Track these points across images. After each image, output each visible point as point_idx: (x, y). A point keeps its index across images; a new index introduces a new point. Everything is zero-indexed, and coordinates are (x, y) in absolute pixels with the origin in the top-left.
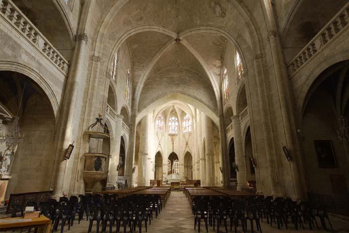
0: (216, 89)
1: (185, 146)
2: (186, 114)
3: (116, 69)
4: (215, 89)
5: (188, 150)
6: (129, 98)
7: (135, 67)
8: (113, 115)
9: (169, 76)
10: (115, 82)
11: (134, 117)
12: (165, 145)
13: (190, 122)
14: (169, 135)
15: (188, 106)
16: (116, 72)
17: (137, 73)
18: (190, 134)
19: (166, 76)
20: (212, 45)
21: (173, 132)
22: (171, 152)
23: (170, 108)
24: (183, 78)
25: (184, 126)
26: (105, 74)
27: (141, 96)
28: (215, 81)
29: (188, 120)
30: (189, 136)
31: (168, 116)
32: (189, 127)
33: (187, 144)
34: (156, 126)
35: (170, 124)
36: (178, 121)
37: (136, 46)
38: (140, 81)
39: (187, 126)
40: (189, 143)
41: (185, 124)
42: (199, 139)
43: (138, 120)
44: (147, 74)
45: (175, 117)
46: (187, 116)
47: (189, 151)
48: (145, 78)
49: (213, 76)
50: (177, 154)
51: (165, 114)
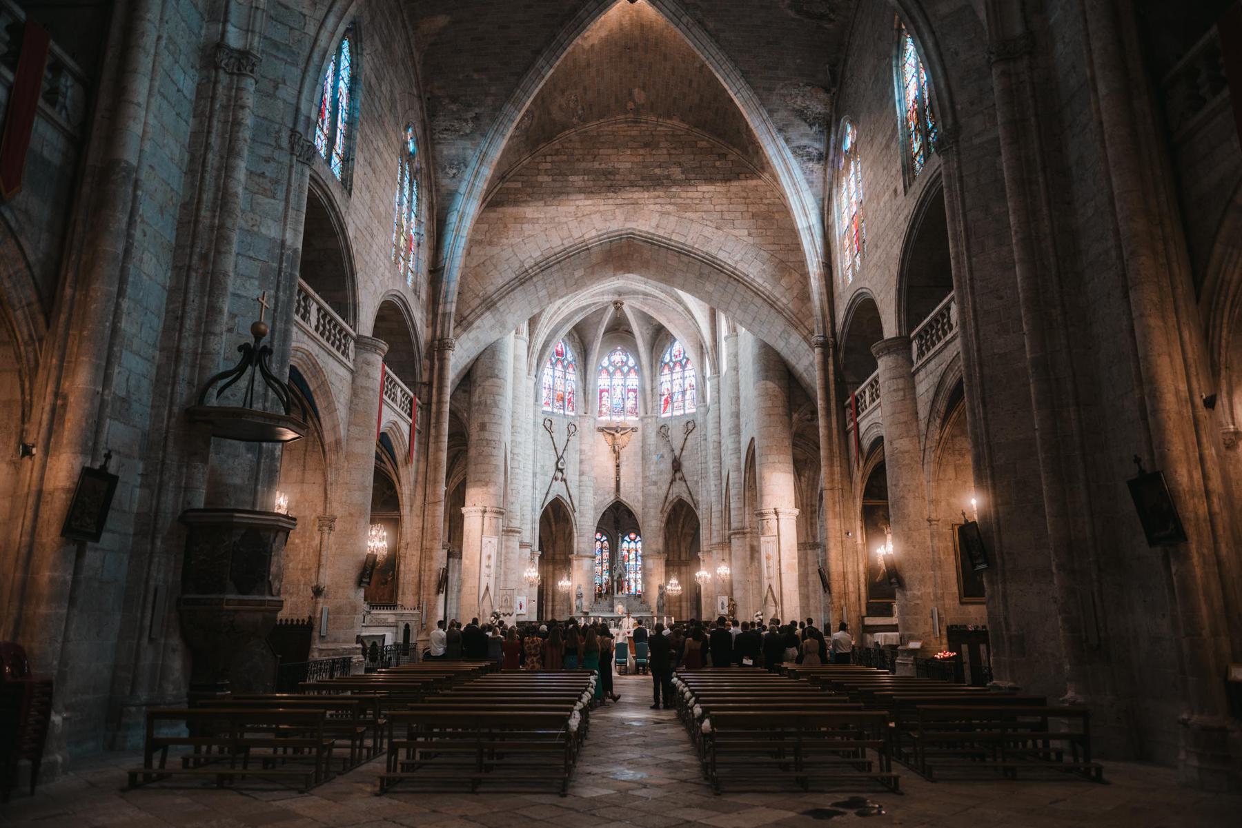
0: (805, 218)
2: (670, 338)
3: (350, 124)
4: (801, 223)
5: (679, 490)
6: (417, 261)
7: (442, 122)
8: (336, 337)
9: (596, 165)
10: (347, 183)
11: (439, 347)
13: (691, 373)
14: (601, 430)
15: (679, 301)
16: (349, 137)
17: (448, 150)
18: (690, 426)
19: (583, 165)
20: (791, 14)
21: (617, 419)
22: (610, 499)
23: (605, 309)
24: (658, 171)
25: (665, 388)
26: (285, 143)
27: (469, 253)
28: (804, 186)
29: (683, 367)
31: (597, 346)
32: (684, 393)
33: (677, 466)
34: (545, 393)
35: (603, 381)
36: (639, 370)
37: (441, 20)
38: (463, 188)
39: (677, 389)
40: (687, 465)
41: (669, 381)
42: (728, 443)
43: (457, 359)
44: (496, 154)
45: (624, 351)
46: (677, 347)
47: (685, 496)
48: (487, 172)
49: (794, 163)
50: (636, 508)
51: (581, 337)
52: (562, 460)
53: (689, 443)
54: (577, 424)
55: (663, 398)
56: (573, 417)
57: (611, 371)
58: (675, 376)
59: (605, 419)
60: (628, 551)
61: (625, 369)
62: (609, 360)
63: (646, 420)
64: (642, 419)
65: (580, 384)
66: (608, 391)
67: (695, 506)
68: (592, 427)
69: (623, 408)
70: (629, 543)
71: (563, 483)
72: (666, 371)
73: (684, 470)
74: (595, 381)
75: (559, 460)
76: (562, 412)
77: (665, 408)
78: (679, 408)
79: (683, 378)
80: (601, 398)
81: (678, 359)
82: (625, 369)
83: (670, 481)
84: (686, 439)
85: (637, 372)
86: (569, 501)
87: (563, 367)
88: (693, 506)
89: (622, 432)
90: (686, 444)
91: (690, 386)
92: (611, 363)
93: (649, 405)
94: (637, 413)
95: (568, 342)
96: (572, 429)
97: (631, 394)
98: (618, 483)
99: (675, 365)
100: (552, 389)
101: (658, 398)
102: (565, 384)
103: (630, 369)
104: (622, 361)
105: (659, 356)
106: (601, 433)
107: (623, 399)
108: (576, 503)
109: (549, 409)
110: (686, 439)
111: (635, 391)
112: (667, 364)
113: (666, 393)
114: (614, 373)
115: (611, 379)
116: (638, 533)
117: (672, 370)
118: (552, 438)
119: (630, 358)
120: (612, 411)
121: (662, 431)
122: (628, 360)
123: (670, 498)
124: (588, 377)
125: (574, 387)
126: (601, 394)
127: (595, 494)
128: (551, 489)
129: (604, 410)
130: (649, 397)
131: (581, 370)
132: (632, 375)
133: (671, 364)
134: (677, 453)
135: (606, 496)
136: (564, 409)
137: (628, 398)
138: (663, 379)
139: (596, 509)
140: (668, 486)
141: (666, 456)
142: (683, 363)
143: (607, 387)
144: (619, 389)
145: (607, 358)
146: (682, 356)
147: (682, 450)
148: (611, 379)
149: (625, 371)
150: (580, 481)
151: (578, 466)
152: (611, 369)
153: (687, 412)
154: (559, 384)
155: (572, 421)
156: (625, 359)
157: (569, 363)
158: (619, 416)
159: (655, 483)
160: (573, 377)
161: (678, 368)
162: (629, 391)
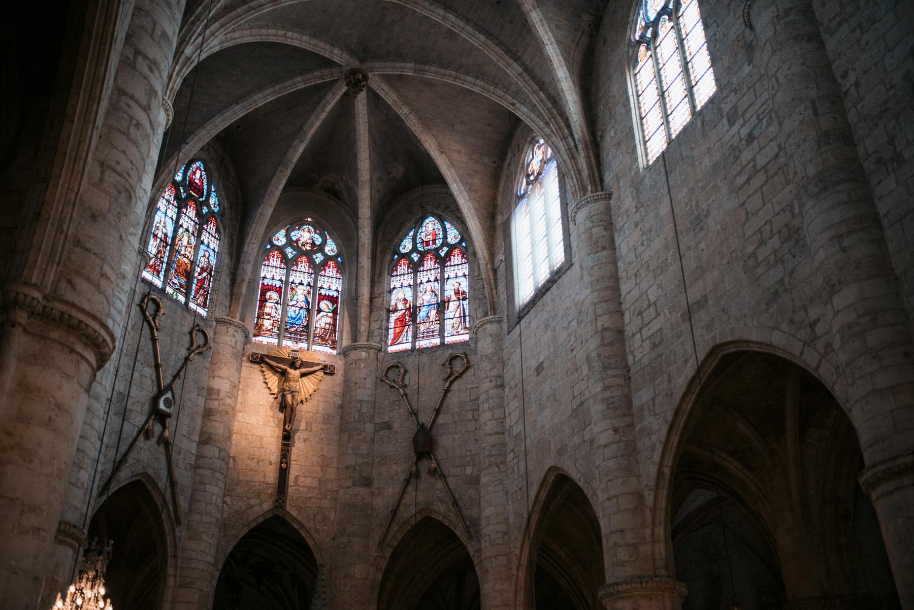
1: (399, 469)
29: (443, 262)
30: (452, 378)
32: (442, 306)
35: (271, 272)
39: (426, 298)
45: (319, 227)
47: (441, 510)
52: (169, 395)
53: (454, 399)
54: (210, 333)
55: (393, 317)
57: (290, 256)
58: (422, 277)
61: (319, 258)
62: (287, 236)
63: (354, 355)
64: (344, 353)
65: (226, 260)
66: (278, 290)
69: (307, 327)
71: (162, 449)
72: (403, 268)
73: (440, 454)
75: (160, 392)
76: (182, 299)
77: (397, 336)
78: (429, 334)
79: (442, 280)
80: (263, 301)
81: (432, 247)
83: (403, 477)
84: (447, 391)
85: (340, 268)
87: (199, 214)
88: (459, 532)
89: (303, 370)
90: (448, 401)
91: (457, 293)
92: (290, 242)
93: (363, 327)
94: (334, 342)
95: (216, 174)
96: (199, 340)
97: (324, 305)
99: (423, 255)
100: (170, 244)
101: (384, 314)
102: (196, 248)
103: (327, 258)
105: (391, 241)
106: (257, 367)
107: (308, 310)
108: (183, 503)
111: (333, 300)
112: (407, 256)
113: (400, 306)
114: (295, 261)
115: (288, 271)
117: (415, 268)
119: (330, 241)
120: (284, 329)
121: (391, 374)
122: (324, 243)
125: (213, 261)
126: (263, 293)
128: (132, 455)
129: (267, 324)
130: (364, 311)
131: (231, 236)
132: (331, 271)
133: (415, 257)
134: (425, 418)
135: (253, 502)
137: (319, 311)
138: (395, 282)
140: (398, 488)
141: (396, 426)
143: (278, 284)
144: (301, 292)
145: (283, 232)
146: (439, 242)
147: (438, 412)
148: (288, 271)
149: (318, 261)
150: (199, 456)
151: (199, 421)
153: (448, 340)
154: (185, 242)
155: (201, 323)
156: (318, 241)
157: (211, 213)
158: (297, 341)
160: (214, 244)
162: (322, 297)
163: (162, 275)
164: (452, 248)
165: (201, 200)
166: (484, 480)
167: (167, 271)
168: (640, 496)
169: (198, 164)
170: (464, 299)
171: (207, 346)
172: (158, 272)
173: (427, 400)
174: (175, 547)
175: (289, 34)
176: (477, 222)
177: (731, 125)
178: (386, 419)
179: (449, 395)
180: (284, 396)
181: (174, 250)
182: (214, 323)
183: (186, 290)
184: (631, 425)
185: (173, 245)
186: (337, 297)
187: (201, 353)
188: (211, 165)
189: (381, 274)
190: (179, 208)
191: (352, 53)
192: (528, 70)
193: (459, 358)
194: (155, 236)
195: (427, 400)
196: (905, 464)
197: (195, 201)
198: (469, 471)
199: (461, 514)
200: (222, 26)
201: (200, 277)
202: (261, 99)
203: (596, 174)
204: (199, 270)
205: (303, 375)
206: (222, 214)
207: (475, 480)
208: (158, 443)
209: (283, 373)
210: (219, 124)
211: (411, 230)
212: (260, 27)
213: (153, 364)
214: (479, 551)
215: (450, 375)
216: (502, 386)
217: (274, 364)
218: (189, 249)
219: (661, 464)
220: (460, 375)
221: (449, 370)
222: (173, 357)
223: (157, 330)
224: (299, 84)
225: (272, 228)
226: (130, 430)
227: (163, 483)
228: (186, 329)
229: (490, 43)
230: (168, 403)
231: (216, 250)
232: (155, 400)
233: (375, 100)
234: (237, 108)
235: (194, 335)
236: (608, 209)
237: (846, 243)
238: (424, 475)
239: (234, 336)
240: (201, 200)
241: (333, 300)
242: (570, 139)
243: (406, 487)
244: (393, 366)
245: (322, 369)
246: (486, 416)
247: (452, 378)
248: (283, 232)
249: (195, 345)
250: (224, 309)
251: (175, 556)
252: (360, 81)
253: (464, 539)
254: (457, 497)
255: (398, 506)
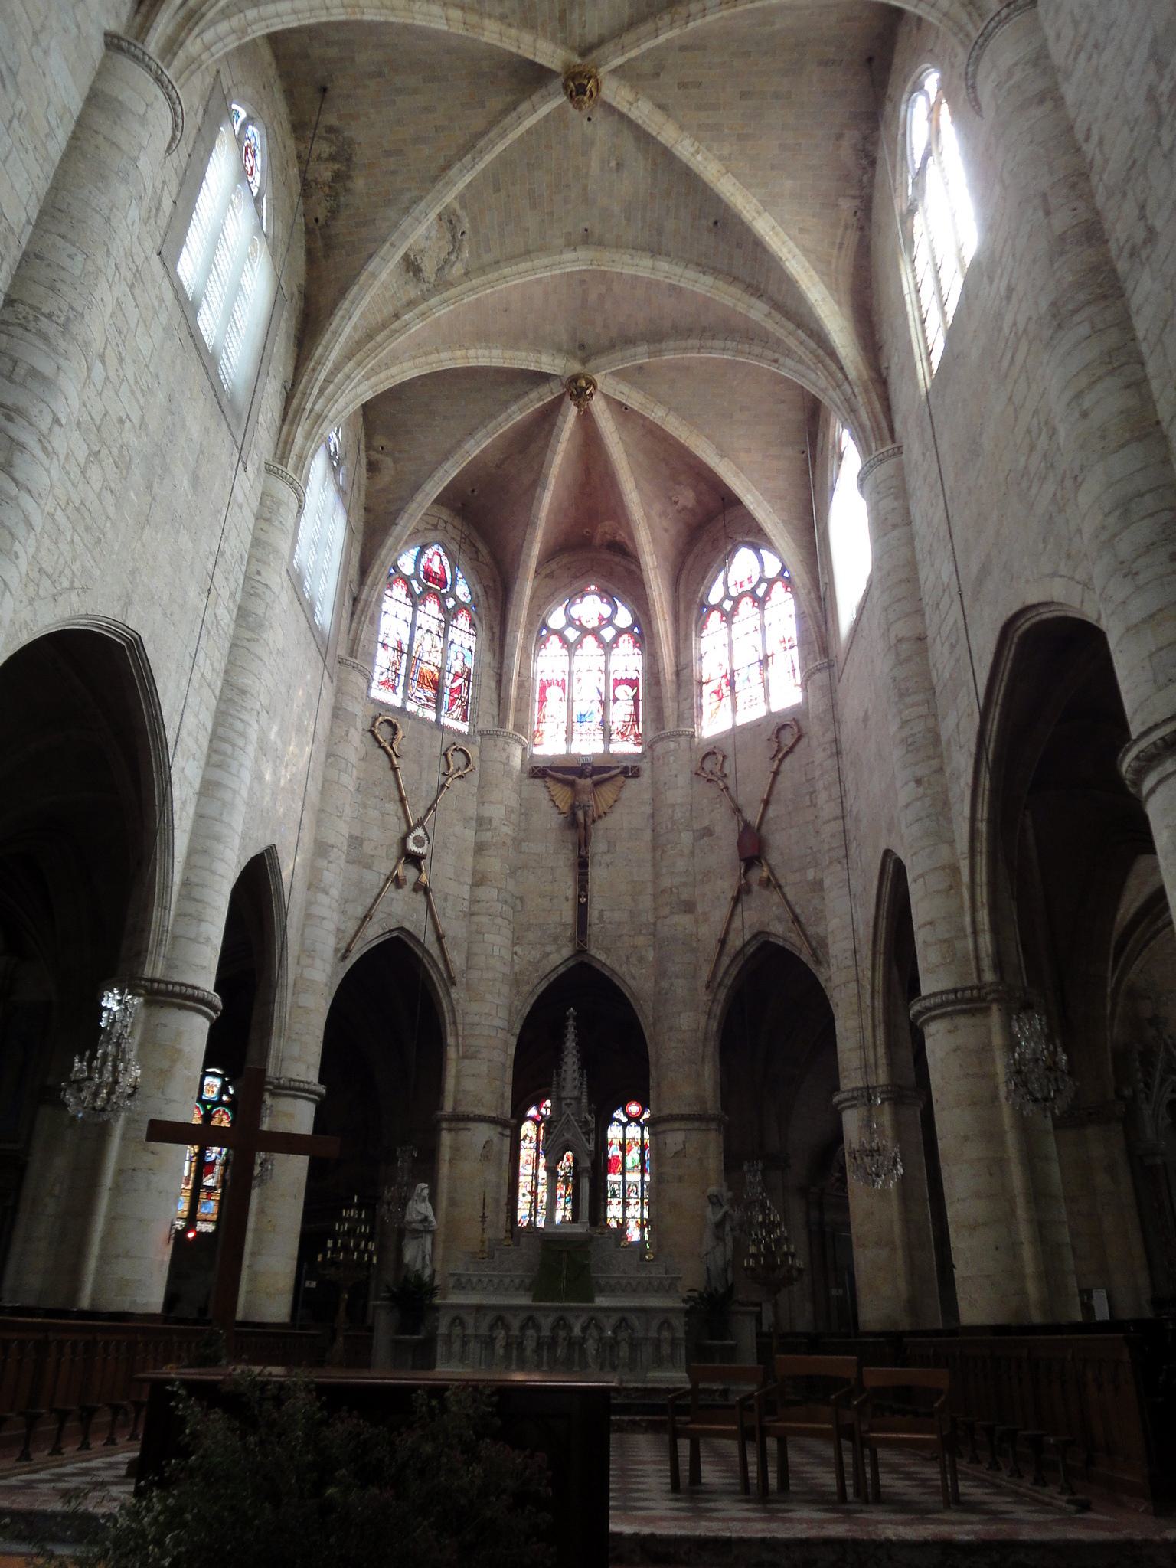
1: (726, 886)
12: (479, 880)
22: (560, 955)
29: (760, 602)
32: (764, 662)
34: (384, 658)
35: (550, 661)
36: (643, 634)
39: (746, 656)
40: (782, 843)
45: (606, 594)
52: (420, 832)
53: (784, 783)
54: (473, 752)
56: (460, 734)
59: (550, 745)
60: (623, 1147)
61: (608, 634)
65: (488, 658)
66: (562, 684)
67: (818, 962)
68: (517, 761)
70: (625, 1125)
71: (421, 897)
73: (774, 857)
74: (527, 657)
75: (410, 830)
76: (431, 715)
80: (543, 700)
81: (748, 587)
82: (608, 634)
83: (731, 893)
84: (776, 773)
86: (434, 950)
87: (443, 609)
88: (805, 957)
90: (779, 786)
92: (571, 622)
96: (457, 760)
98: (582, 910)
99: (737, 601)
103: (620, 632)
104: (601, 618)
105: (696, 592)
106: (538, 782)
108: (457, 959)
109: (395, 700)
110: (776, 773)
111: (632, 683)
112: (718, 607)
114: (579, 642)
116: (645, 1106)
117: (728, 617)
118: (394, 769)
123: (736, 942)
124: (508, 639)
125: (470, 664)
127: (517, 940)
132: (626, 644)
134: (752, 815)
135: (549, 949)
136: (438, 710)
137: (615, 700)
139: (516, 982)
140: (726, 910)
141: (718, 830)
142: (760, 592)
145: (561, 610)
146: (755, 580)
147: (766, 803)
150: (474, 901)
151: (469, 860)
152: (572, 634)
154: (427, 646)
156: (606, 611)
157: (460, 606)
159: (689, 907)
160: (470, 642)
161: (746, 604)
162: (618, 682)
163: (399, 690)
164: (771, 583)
165: (444, 591)
166: (827, 883)
167: (406, 686)
168: (955, 869)
169: (435, 548)
170: (792, 647)
171: (470, 767)
172: (394, 688)
173: (750, 793)
174: (453, 1011)
175: (472, 352)
176: (788, 539)
177: (991, 282)
178: (706, 823)
179: (779, 778)
180: (574, 814)
181: (413, 660)
182: (478, 738)
183: (436, 703)
184: (940, 770)
185: (409, 654)
186: (637, 679)
187: (460, 777)
188: (453, 547)
189: (688, 637)
190: (414, 606)
191: (569, 354)
192: (777, 306)
193: (788, 728)
194: (385, 646)
195: (750, 793)
196: (1162, 739)
197: (436, 594)
198: (811, 874)
199: (805, 935)
200: (359, 364)
201: (455, 685)
202: (476, 447)
203: (884, 424)
204: (451, 677)
205: (597, 784)
206: (475, 603)
207: (817, 886)
208: (415, 890)
209: (571, 784)
210: (434, 488)
211: (720, 572)
212: (426, 354)
213: (397, 797)
214: (829, 979)
215: (778, 751)
216: (838, 753)
217: (560, 775)
218: (435, 654)
219: (973, 819)
220: (791, 749)
221: (775, 746)
222: (425, 785)
223: (397, 756)
224: (518, 414)
225: (541, 605)
226: (374, 878)
227: (429, 939)
228: (438, 751)
229: (720, 284)
230: (419, 842)
231: (473, 649)
232: (404, 841)
233: (621, 409)
234: (447, 466)
235: (450, 756)
236: (900, 468)
237: (1087, 402)
238: (755, 888)
239: (504, 749)
240: (444, 591)
241: (632, 683)
242: (846, 386)
243: (734, 908)
244: (708, 754)
245: (621, 773)
246: (822, 797)
247: (780, 756)
248: (561, 610)
249: (452, 768)
250: (490, 719)
251: (455, 1023)
252: (584, 390)
253: (812, 966)
254: (798, 911)
255: (727, 932)
